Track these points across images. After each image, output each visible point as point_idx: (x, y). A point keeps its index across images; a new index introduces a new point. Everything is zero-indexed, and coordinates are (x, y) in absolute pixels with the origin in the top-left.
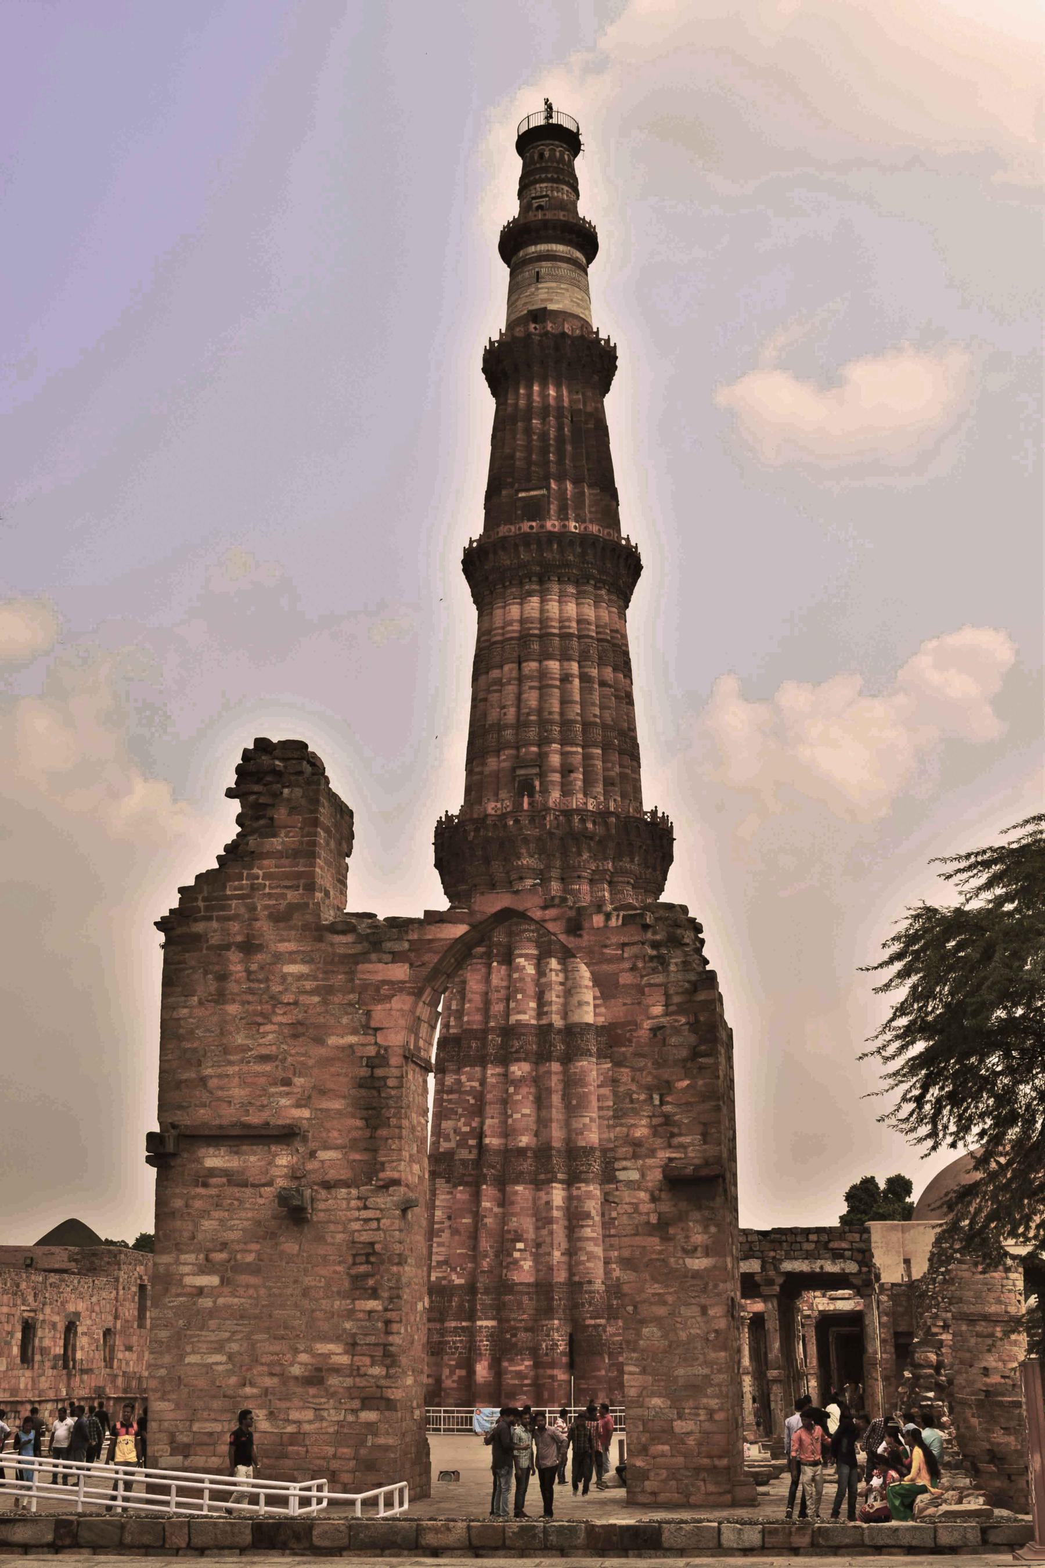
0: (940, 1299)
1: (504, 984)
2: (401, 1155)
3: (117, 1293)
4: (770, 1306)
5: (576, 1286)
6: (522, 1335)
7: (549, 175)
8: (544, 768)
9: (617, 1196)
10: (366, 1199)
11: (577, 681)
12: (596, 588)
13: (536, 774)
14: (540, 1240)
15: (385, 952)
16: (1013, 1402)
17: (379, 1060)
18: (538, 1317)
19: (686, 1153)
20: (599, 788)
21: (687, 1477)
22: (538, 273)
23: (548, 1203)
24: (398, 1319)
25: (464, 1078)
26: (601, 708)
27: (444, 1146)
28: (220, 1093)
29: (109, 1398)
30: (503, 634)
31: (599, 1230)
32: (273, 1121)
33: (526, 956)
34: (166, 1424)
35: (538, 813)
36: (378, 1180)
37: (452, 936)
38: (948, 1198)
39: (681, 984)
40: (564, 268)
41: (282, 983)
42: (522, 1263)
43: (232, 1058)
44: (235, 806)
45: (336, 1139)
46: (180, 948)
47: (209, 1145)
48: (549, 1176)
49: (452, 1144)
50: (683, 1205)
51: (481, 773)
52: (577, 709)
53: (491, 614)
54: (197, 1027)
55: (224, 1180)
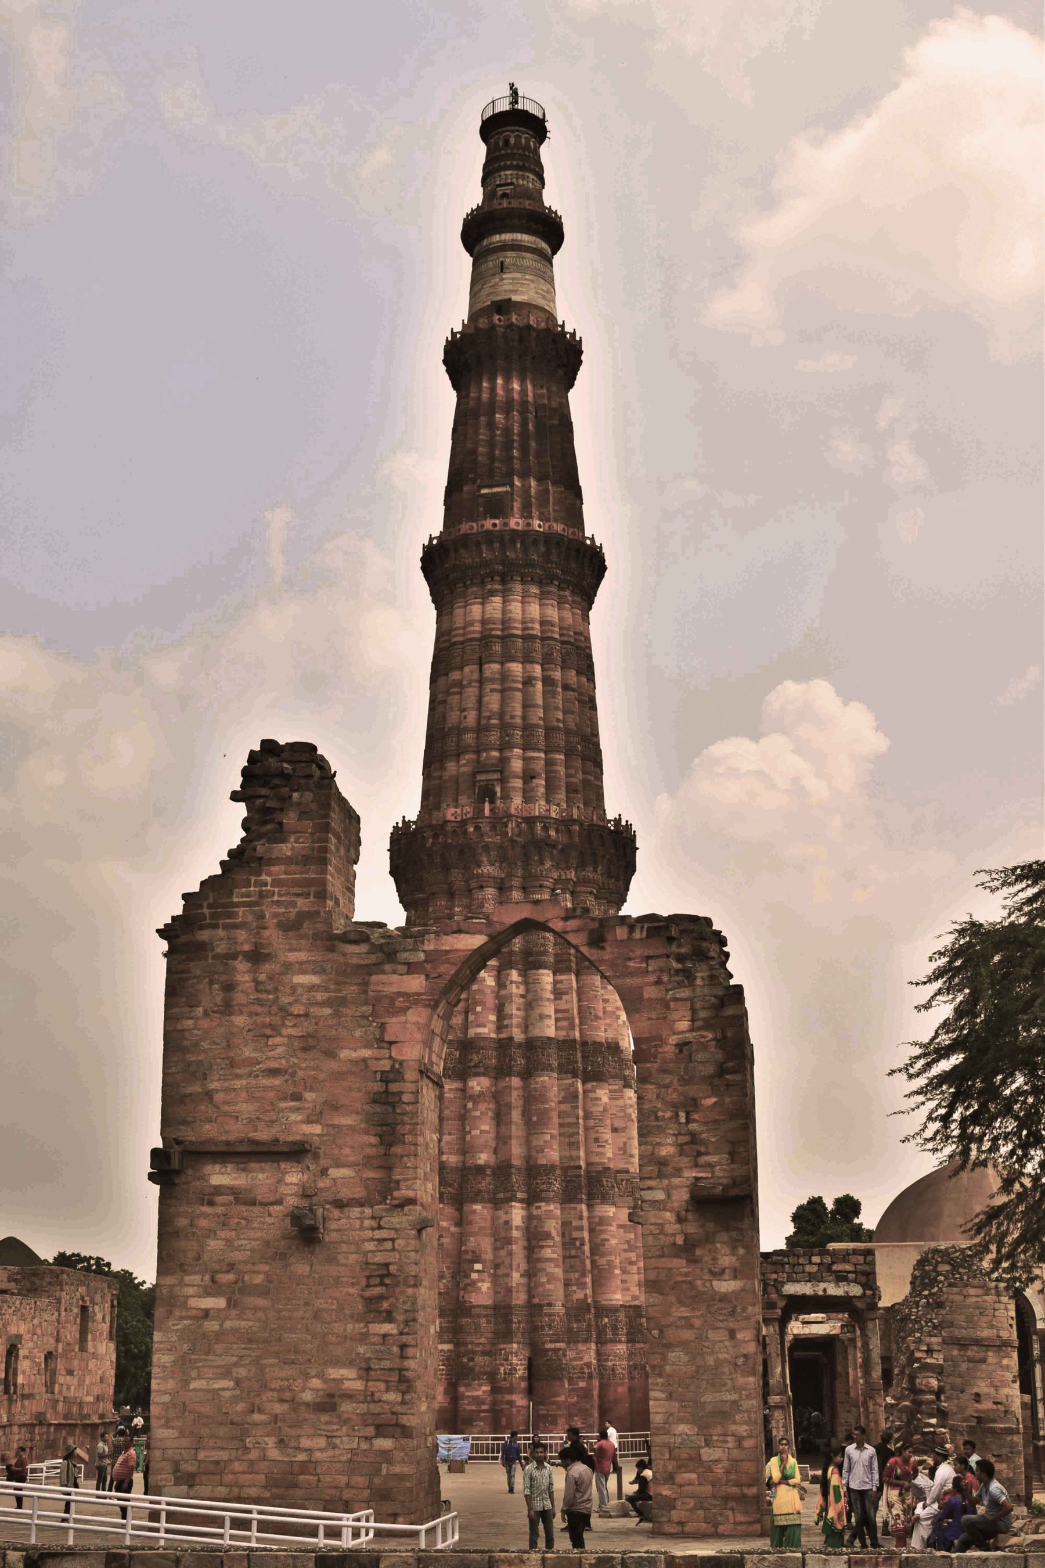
0: (923, 1323)
2: (416, 1173)
3: (59, 1315)
4: (771, 1329)
5: (535, 1309)
6: (479, 1359)
7: (515, 163)
8: (506, 774)
9: (641, 1217)
10: (380, 1218)
11: (539, 685)
12: (560, 588)
13: (497, 780)
14: (498, 1261)
15: (400, 963)
16: (1005, 1428)
17: (393, 1074)
18: (496, 1341)
19: (713, 1172)
20: (561, 796)
21: (716, 1506)
22: (502, 263)
23: (507, 1223)
24: (413, 1343)
26: (565, 713)
28: (226, 1108)
29: (50, 1425)
30: (464, 635)
31: (560, 1251)
32: (283, 1138)
34: (170, 1452)
35: (499, 821)
36: (393, 1198)
37: (469, 947)
38: (977, 1220)
39: (707, 998)
41: (293, 994)
43: (239, 1071)
44: (241, 810)
45: (347, 1156)
46: (184, 957)
47: (215, 1162)
48: (509, 1195)
50: (710, 1226)
51: (440, 778)
53: (451, 613)
54: (203, 1039)
55: (231, 1198)
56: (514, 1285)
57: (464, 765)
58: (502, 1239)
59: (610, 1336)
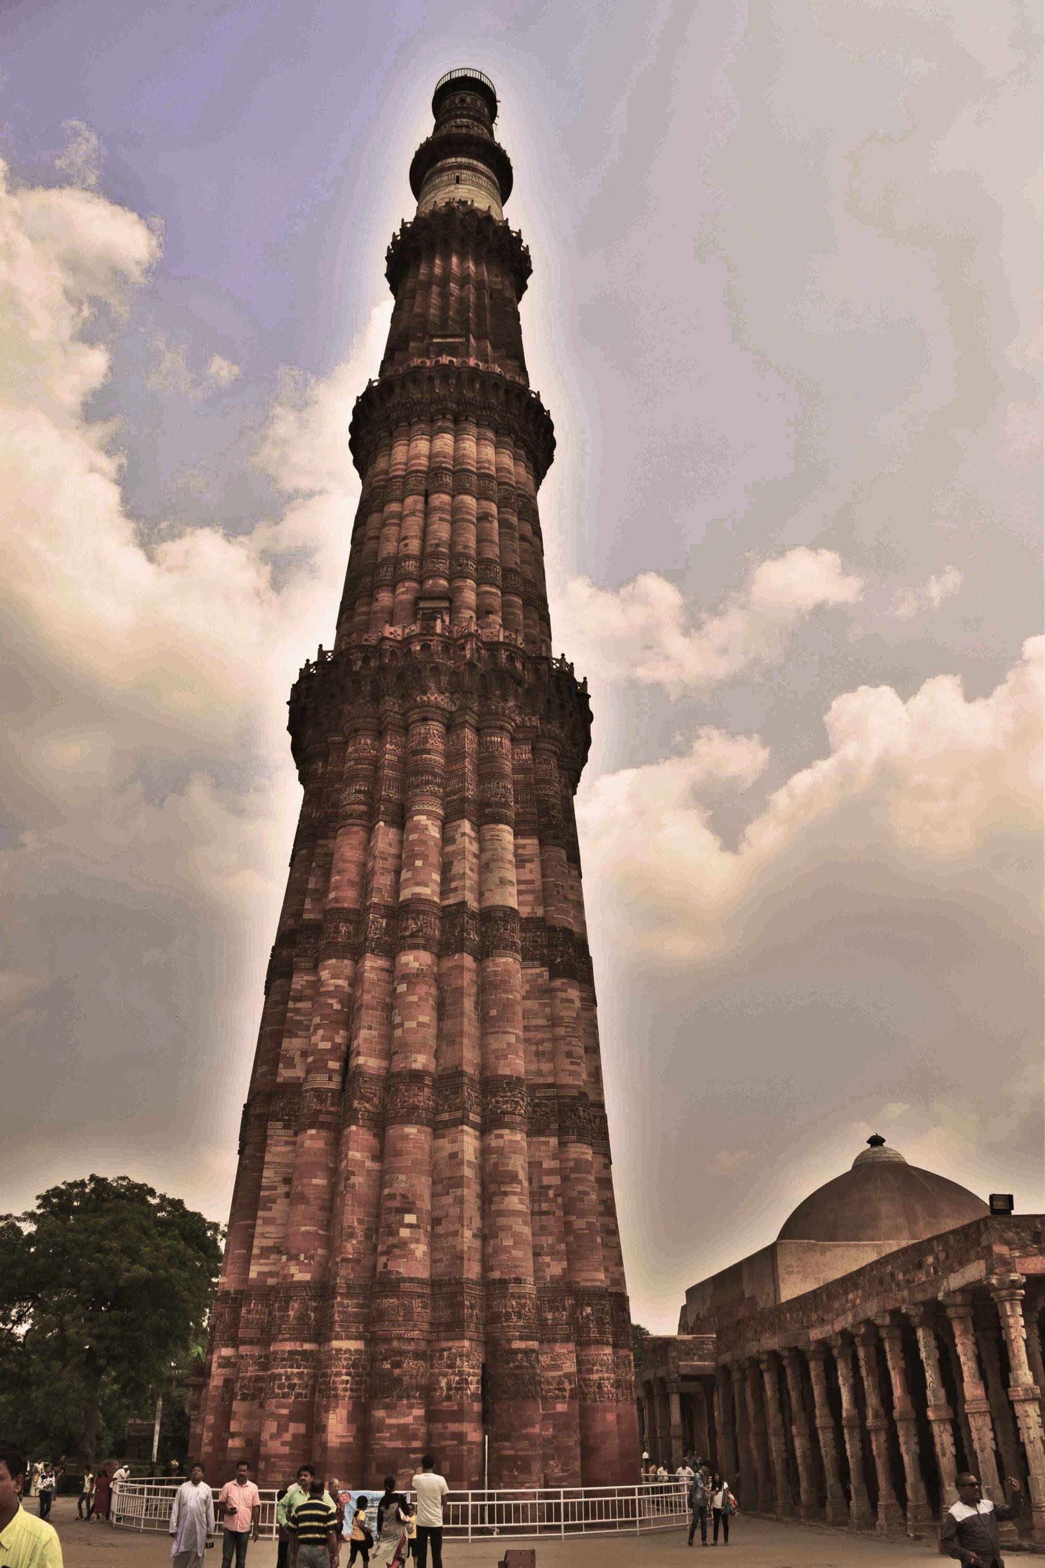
1: (393, 851)
5: (494, 1288)
6: (409, 1364)
11: (496, 524)
12: (516, 446)
13: (446, 608)
18: (434, 1336)
22: (458, 177)
23: (454, 1156)
25: (325, 974)
26: (523, 562)
27: (285, 1074)
30: (405, 470)
31: (527, 1199)
33: (429, 814)
40: (484, 181)
42: (413, 1246)
48: (459, 1114)
49: (298, 1072)
52: (497, 550)
53: (390, 455)
56: (465, 1249)
57: (403, 593)
58: (445, 1181)
59: (594, 1334)
